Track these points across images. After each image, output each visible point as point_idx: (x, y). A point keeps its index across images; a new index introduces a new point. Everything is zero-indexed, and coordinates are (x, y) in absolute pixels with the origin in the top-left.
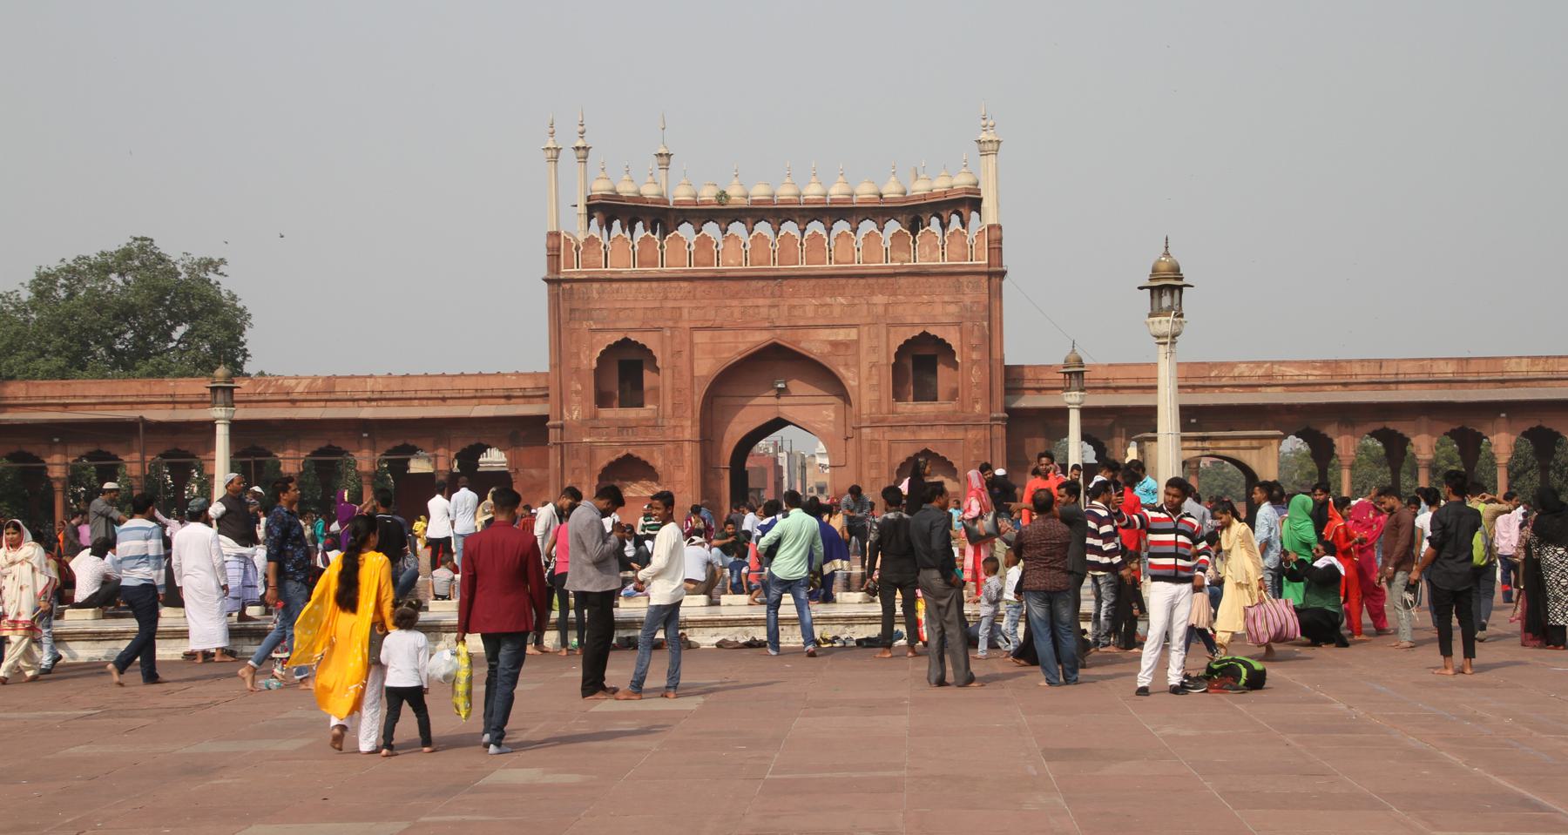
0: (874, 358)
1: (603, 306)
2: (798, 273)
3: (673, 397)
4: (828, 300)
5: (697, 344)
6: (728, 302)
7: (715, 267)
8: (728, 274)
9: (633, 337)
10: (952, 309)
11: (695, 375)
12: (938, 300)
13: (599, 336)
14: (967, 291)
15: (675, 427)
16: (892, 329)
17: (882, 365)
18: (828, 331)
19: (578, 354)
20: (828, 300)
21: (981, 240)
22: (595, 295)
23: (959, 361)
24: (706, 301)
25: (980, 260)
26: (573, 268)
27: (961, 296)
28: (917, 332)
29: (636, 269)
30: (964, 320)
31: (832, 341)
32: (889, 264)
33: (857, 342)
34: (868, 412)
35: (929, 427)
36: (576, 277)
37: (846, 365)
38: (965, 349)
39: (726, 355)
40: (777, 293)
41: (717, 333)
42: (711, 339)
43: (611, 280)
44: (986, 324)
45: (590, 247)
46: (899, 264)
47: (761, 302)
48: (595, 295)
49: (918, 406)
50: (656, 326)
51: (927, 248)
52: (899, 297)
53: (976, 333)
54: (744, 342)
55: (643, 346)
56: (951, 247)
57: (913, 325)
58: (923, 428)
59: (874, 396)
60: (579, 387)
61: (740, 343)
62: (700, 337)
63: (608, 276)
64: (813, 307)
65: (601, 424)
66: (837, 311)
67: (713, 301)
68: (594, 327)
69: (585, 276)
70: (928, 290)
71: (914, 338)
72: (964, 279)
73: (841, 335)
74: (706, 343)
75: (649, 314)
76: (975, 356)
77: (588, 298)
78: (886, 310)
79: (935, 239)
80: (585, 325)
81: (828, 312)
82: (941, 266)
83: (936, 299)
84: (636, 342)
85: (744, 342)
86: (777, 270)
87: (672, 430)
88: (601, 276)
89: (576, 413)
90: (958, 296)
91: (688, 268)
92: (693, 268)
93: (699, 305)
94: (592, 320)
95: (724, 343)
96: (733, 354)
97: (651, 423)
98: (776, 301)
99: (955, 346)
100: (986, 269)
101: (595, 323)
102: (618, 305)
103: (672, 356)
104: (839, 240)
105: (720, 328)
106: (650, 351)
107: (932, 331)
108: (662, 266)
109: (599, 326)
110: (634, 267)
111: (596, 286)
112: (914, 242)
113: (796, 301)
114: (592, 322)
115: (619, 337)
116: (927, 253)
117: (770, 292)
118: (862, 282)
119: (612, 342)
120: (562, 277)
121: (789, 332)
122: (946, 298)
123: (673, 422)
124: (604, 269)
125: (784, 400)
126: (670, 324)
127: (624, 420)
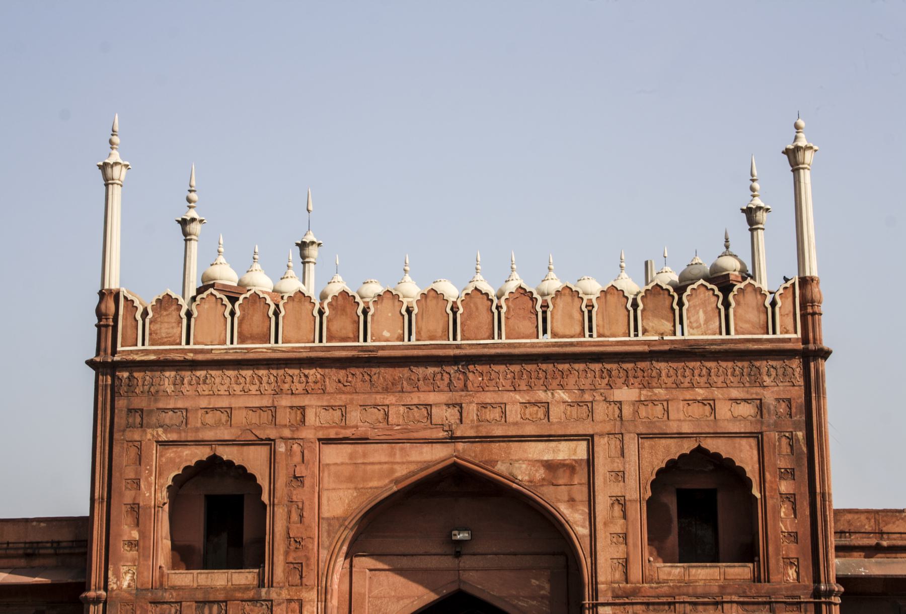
0: (617, 489)
1: (180, 404)
2: (493, 351)
3: (287, 553)
4: (542, 395)
5: (328, 465)
6: (379, 398)
7: (361, 343)
8: (381, 353)
9: (226, 453)
10: (746, 410)
11: (325, 514)
12: (720, 396)
13: (171, 453)
14: (768, 381)
15: (289, 601)
16: (647, 443)
17: (630, 501)
18: (541, 446)
19: (136, 483)
20: (542, 395)
21: (790, 299)
22: (170, 389)
23: (758, 495)
24: (343, 396)
25: (787, 332)
26: (136, 345)
27: (759, 390)
28: (687, 447)
29: (235, 345)
30: (764, 429)
31: (547, 461)
32: (641, 337)
33: (590, 463)
34: (609, 578)
35: (711, 607)
36: (138, 358)
37: (572, 501)
38: (768, 475)
39: (374, 484)
40: (459, 384)
41: (360, 448)
42: (352, 456)
43: (193, 365)
44: (800, 435)
45: (165, 313)
46: (656, 338)
47: (432, 398)
48: (170, 389)
49: (693, 571)
50: (263, 436)
51: (701, 313)
52: (656, 391)
53: (786, 449)
54: (403, 463)
55: (242, 468)
56: (740, 311)
57: (681, 436)
58: (700, 608)
59: (619, 552)
60: (135, 535)
61: (398, 463)
62: (333, 455)
63: (190, 356)
64: (518, 407)
65: (167, 596)
66: (556, 412)
67: (355, 396)
68: (164, 437)
69: (152, 357)
70: (704, 379)
71: (683, 456)
72: (763, 365)
73: (564, 452)
74: (342, 464)
75: (254, 418)
76: (785, 487)
77: (157, 392)
78: (636, 412)
79: (714, 299)
80: (149, 434)
81: (541, 414)
82: (723, 341)
83: (717, 393)
84: (230, 463)
85: (403, 463)
86: (458, 347)
87: (284, 606)
88: (178, 357)
89: (128, 577)
90: (754, 390)
91: (317, 344)
92: (325, 343)
93: (333, 403)
94: (162, 427)
95: (373, 464)
96: (387, 481)
97: (250, 594)
98: (456, 396)
99: (751, 470)
100: (800, 346)
101: (165, 431)
102: (204, 403)
103: (288, 484)
104: (560, 302)
105: (363, 440)
106: (252, 478)
107: (712, 445)
108: (276, 342)
109: (173, 437)
110: (232, 343)
111: (170, 374)
112: (681, 304)
113: (488, 398)
114: (160, 430)
115: (203, 453)
116: (702, 321)
117: (447, 381)
118: (597, 367)
119: (193, 463)
120: (117, 358)
121: (478, 447)
122: (735, 393)
123: (285, 594)
124: (184, 346)
125: (466, 561)
126: (287, 433)
127: (207, 590)
